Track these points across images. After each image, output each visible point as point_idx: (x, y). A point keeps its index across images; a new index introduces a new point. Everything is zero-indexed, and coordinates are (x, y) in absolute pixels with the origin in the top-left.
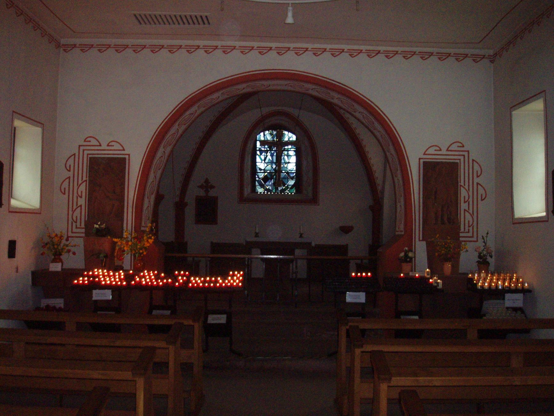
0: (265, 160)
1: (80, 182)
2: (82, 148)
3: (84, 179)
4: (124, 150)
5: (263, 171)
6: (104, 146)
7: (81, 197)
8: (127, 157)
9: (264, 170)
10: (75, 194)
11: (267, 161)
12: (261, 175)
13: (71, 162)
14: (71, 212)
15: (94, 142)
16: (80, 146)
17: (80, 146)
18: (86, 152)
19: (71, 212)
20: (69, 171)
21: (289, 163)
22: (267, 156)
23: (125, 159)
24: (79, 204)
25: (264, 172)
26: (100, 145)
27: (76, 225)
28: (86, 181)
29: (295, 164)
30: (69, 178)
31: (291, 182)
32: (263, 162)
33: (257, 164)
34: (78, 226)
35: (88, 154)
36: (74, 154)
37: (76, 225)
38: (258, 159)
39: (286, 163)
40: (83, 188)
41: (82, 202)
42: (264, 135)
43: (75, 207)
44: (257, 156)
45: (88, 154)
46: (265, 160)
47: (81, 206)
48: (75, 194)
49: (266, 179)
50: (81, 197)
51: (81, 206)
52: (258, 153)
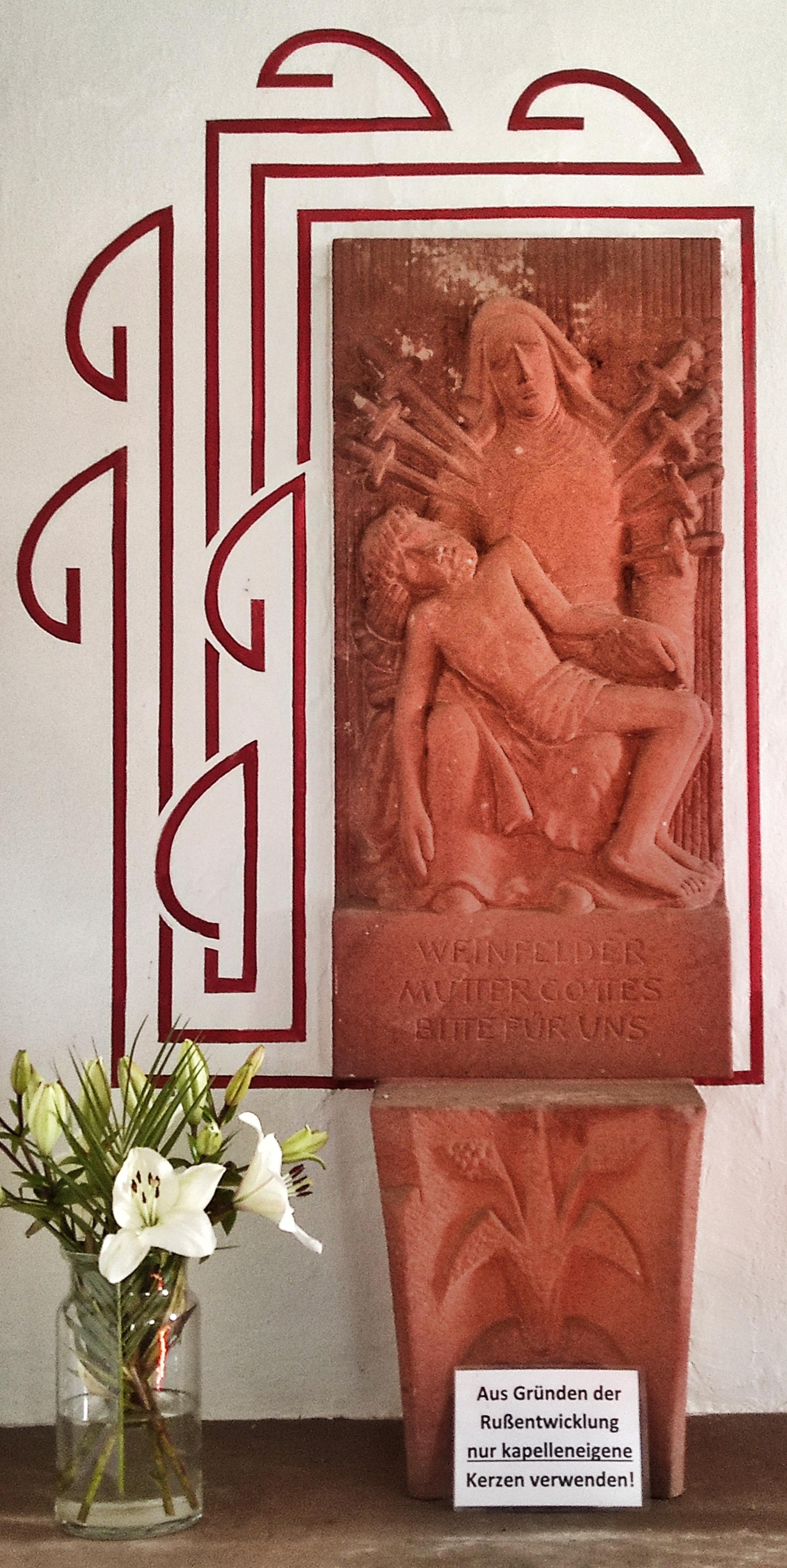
1: (236, 500)
2: (239, 153)
3: (280, 468)
6: (478, 130)
7: (254, 658)
10: (192, 632)
13: (126, 296)
14: (146, 821)
17: (215, 129)
18: (285, 198)
19: (146, 821)
20: (115, 388)
23: (710, 248)
24: (228, 747)
27: (211, 957)
30: (117, 462)
34: (231, 967)
35: (306, 219)
36: (162, 220)
37: (211, 957)
40: (261, 567)
41: (256, 707)
43: (190, 765)
45: (306, 219)
47: (248, 757)
48: (192, 632)
50: (254, 658)
51: (248, 757)
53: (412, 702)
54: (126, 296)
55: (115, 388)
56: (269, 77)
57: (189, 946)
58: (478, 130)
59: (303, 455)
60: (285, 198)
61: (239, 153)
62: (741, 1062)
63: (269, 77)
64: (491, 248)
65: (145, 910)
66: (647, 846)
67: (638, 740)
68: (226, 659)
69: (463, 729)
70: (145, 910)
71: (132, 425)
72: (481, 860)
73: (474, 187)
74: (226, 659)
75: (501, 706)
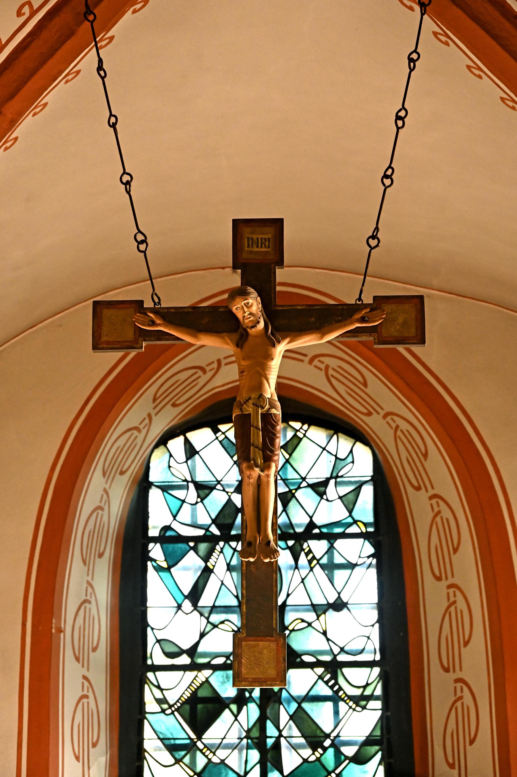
0: (195, 595)
5: (185, 660)
9: (192, 652)
11: (206, 600)
12: (176, 685)
21: (339, 605)
22: (207, 572)
25: (194, 667)
29: (374, 615)
31: (361, 724)
32: (187, 605)
33: (152, 617)
38: (158, 592)
39: (319, 610)
42: (191, 452)
44: (151, 574)
46: (195, 595)
49: (201, 710)
52: (156, 551)
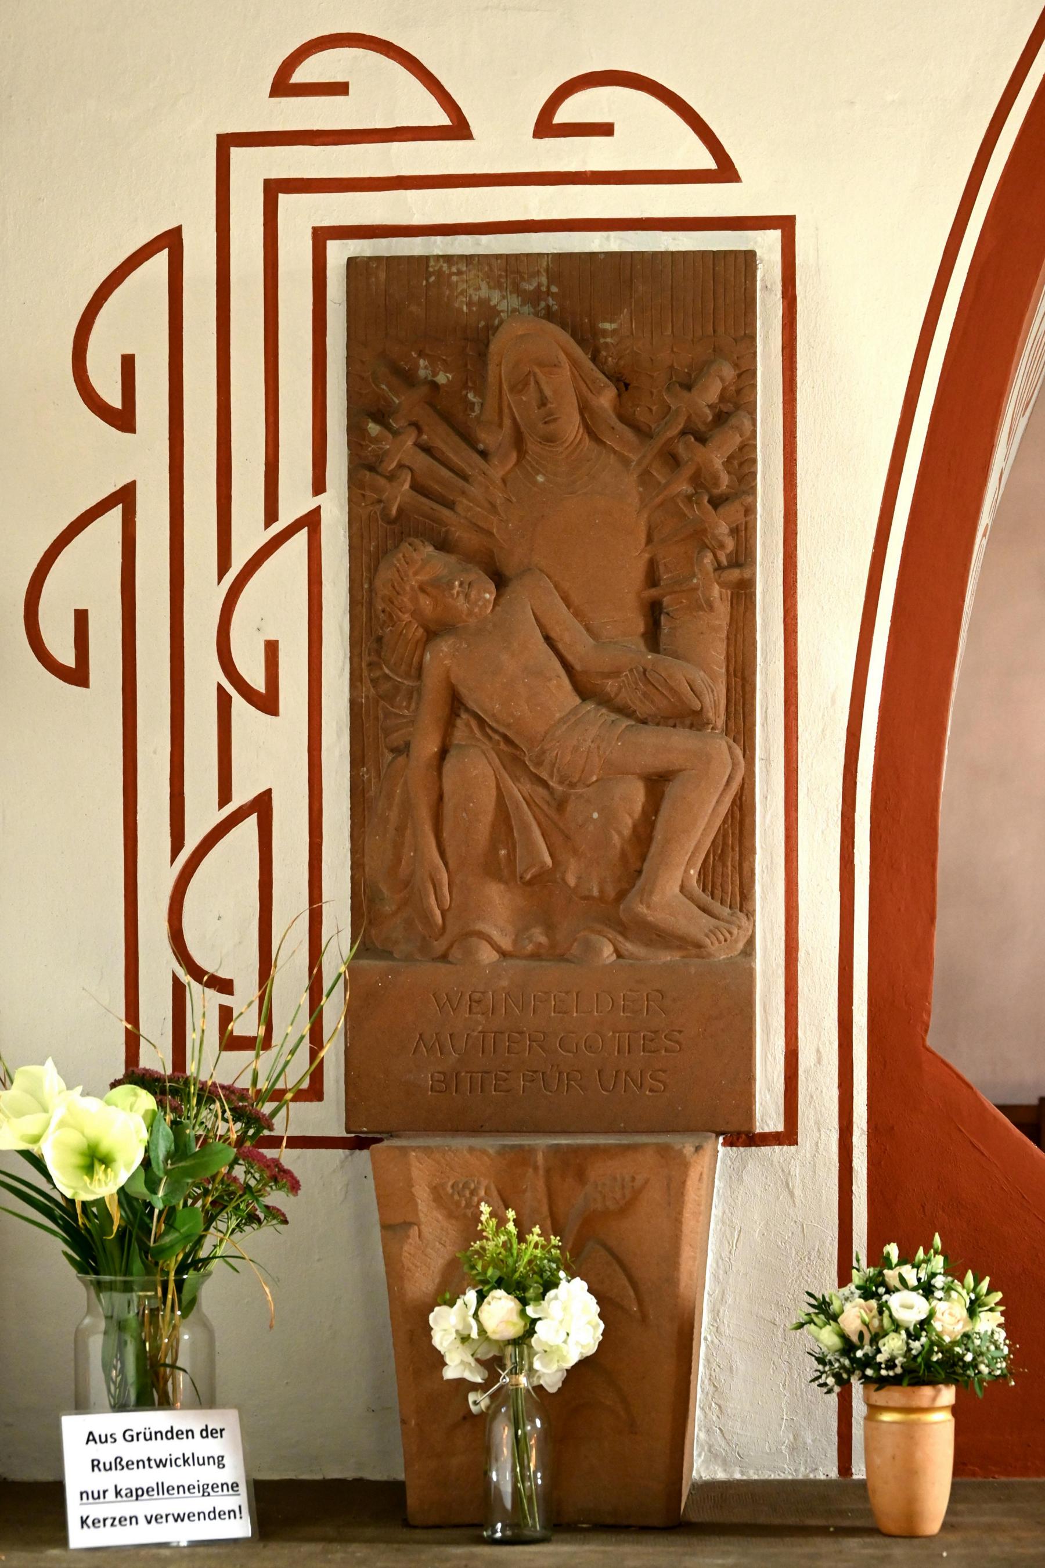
1: (249, 534)
2: (251, 168)
4: (725, 171)
6: (502, 138)
7: (267, 702)
8: (766, 245)
10: (204, 675)
13: (136, 321)
14: (157, 874)
15: (385, 95)
16: (226, 143)
17: (226, 143)
18: (299, 215)
19: (157, 874)
20: (123, 419)
24: (241, 796)
26: (459, 129)
27: (226, 1015)
28: (311, 521)
35: (321, 236)
36: (171, 241)
37: (226, 1015)
41: (271, 753)
45: (321, 236)
47: (262, 806)
48: (204, 675)
50: (267, 702)
51: (262, 806)
53: (428, 746)
54: (136, 321)
55: (123, 419)
56: (283, 86)
57: (204, 1004)
58: (502, 138)
59: (319, 486)
60: (299, 215)
61: (251, 168)
62: (768, 1115)
63: (283, 86)
64: (513, 266)
65: (158, 965)
66: (671, 890)
67: (657, 783)
68: (238, 702)
69: (477, 773)
70: (158, 965)
71: (142, 460)
72: (498, 912)
73: (503, 192)
74: (238, 702)
75: (513, 752)
